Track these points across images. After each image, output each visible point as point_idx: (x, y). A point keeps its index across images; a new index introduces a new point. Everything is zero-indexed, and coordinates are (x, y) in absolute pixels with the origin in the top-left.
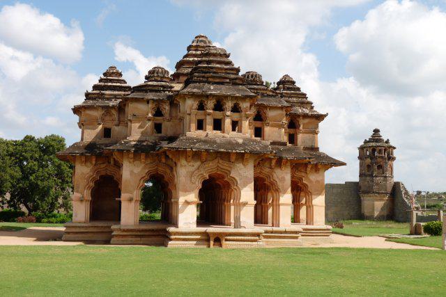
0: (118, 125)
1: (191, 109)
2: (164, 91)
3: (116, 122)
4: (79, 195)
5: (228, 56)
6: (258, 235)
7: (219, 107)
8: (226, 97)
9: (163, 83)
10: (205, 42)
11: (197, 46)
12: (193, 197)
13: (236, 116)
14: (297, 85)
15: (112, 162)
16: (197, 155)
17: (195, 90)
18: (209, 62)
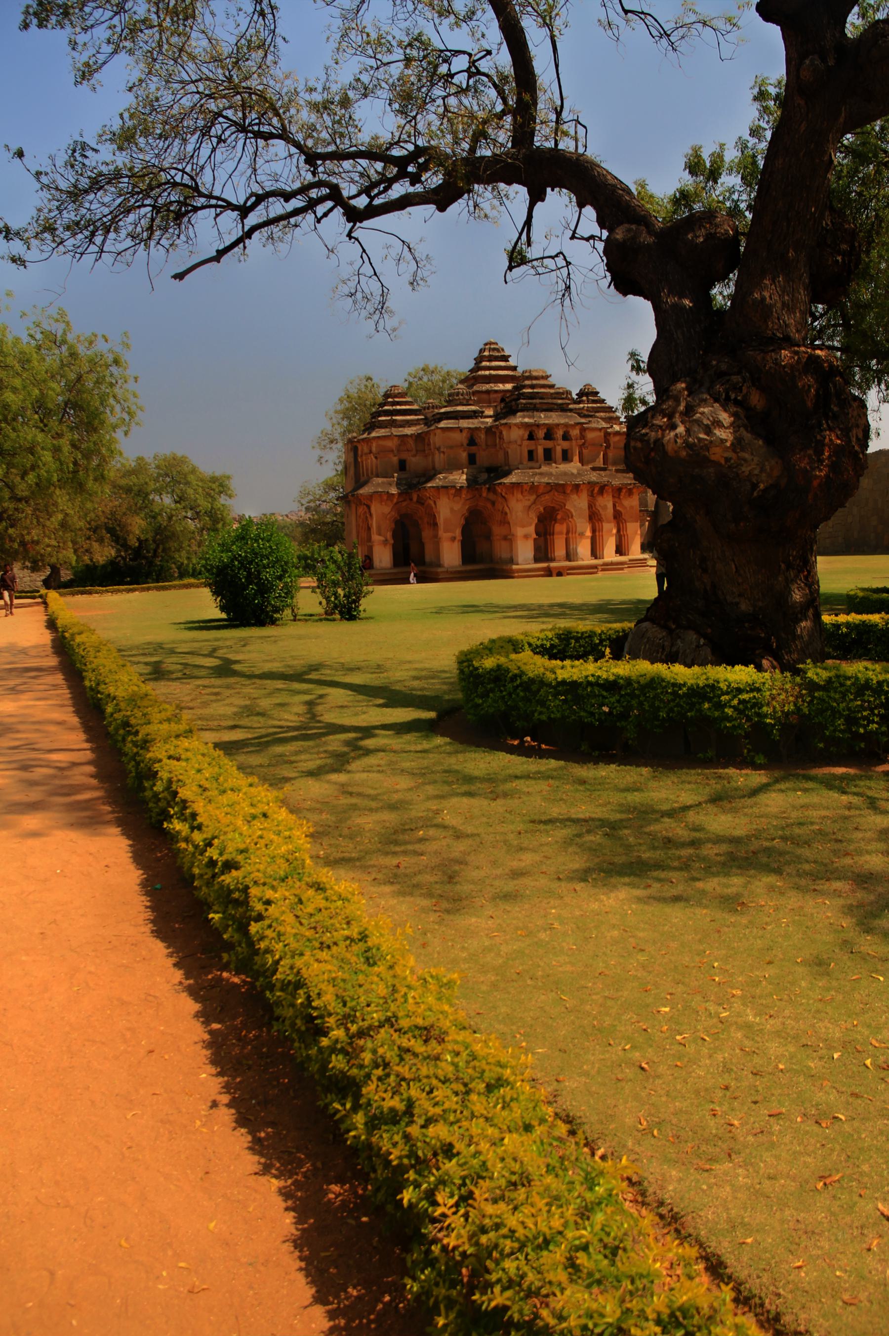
0: (415, 456)
1: (522, 440)
2: (476, 417)
3: (414, 452)
4: (382, 538)
5: (547, 377)
6: (595, 567)
7: (549, 436)
8: (558, 425)
9: (473, 408)
10: (498, 350)
11: (490, 356)
12: (531, 530)
13: (565, 445)
14: (602, 395)
15: (415, 498)
16: (533, 488)
17: (526, 420)
18: (533, 387)
